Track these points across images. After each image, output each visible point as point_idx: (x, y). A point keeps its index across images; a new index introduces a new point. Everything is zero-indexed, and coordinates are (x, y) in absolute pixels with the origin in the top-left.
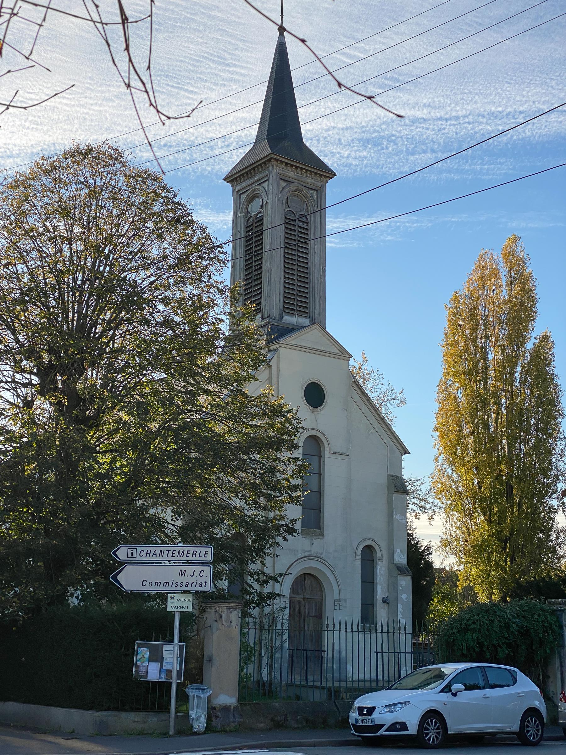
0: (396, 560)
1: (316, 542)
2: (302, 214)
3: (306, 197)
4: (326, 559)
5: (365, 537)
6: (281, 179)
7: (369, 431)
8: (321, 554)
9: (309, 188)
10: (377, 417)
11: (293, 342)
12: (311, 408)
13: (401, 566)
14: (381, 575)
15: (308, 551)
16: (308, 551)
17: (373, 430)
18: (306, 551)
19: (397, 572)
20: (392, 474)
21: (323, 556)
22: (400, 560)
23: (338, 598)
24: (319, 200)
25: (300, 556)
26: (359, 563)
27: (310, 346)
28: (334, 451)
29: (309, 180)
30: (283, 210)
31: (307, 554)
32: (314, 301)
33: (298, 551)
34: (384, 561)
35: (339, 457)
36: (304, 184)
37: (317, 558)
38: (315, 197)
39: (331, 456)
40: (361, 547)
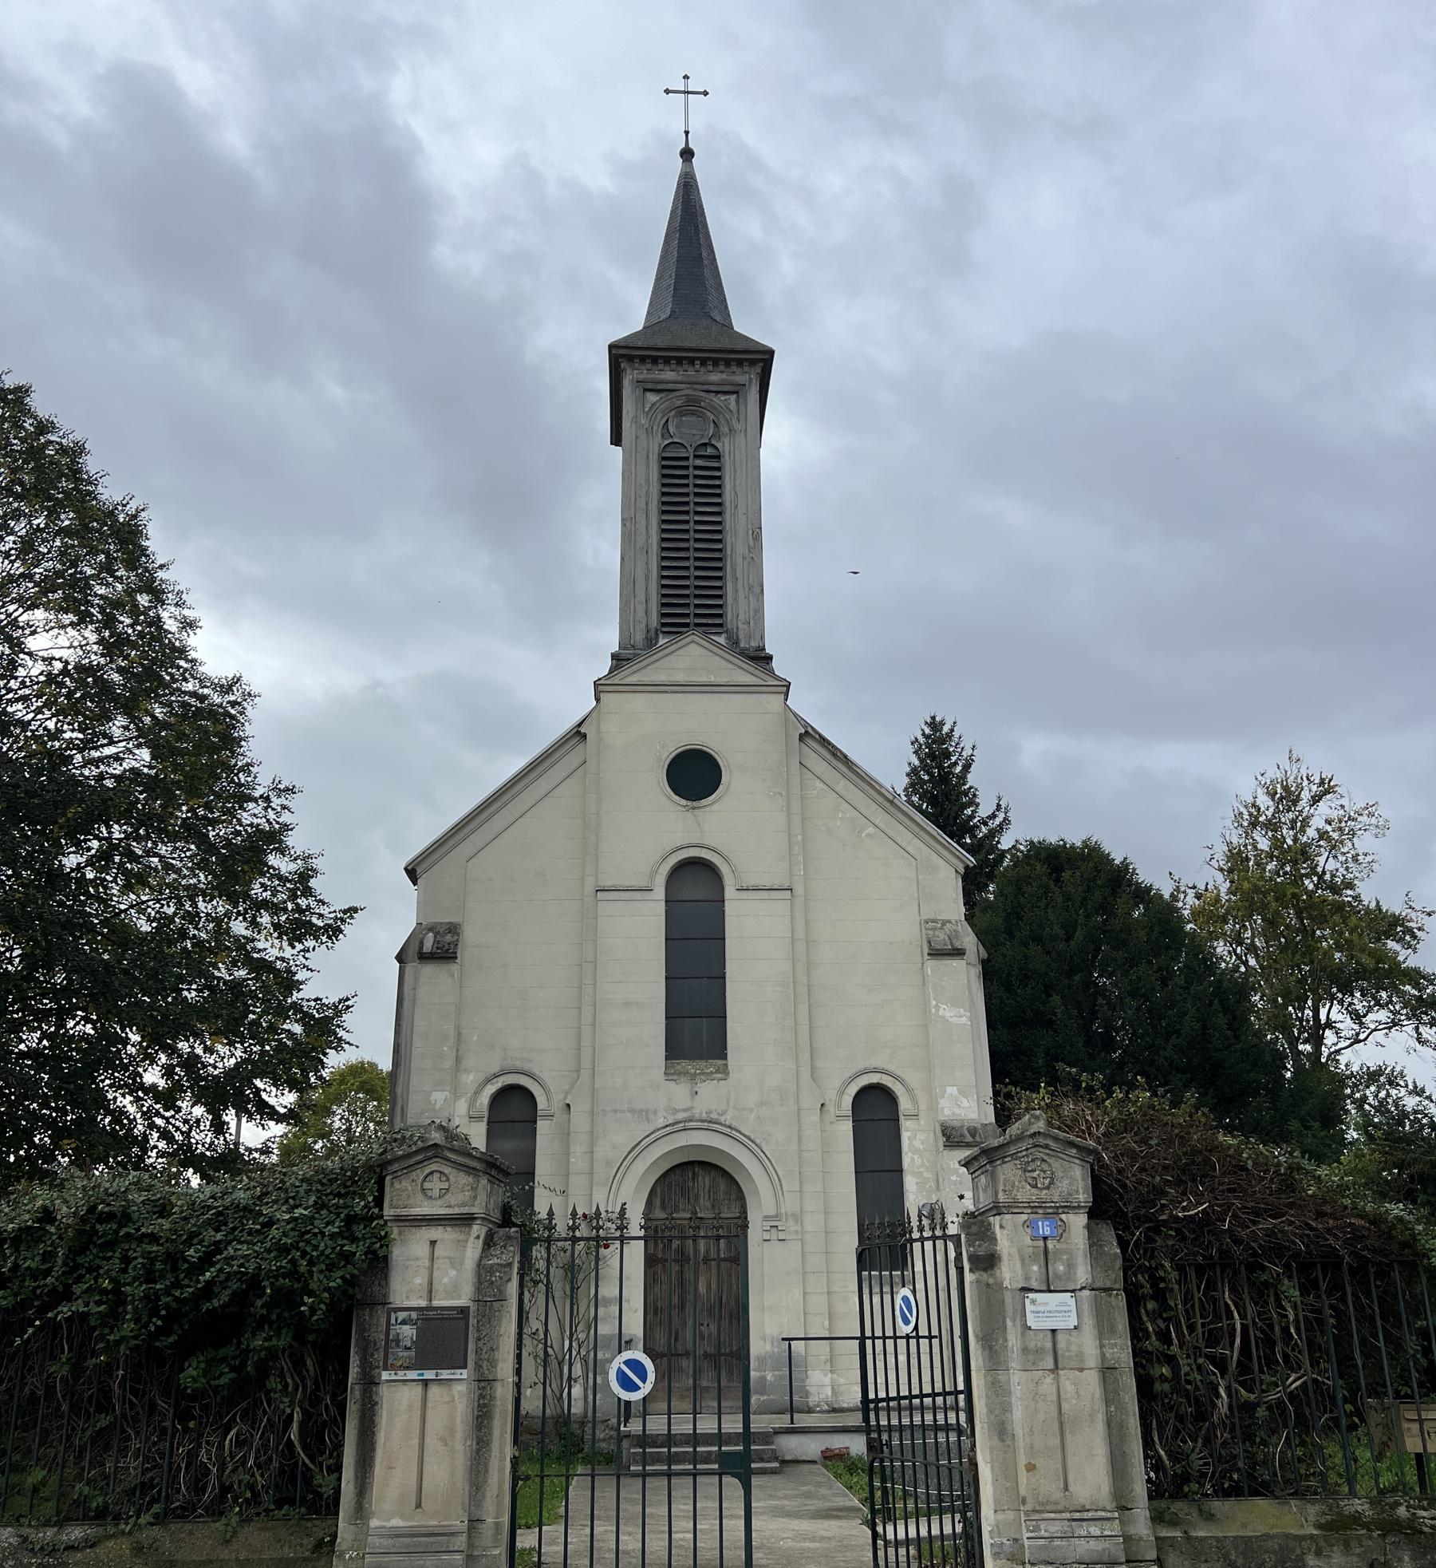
0: (947, 1112)
1: (706, 1089)
2: (705, 445)
3: (713, 409)
4: (735, 1124)
5: (861, 1065)
6: (645, 390)
7: (861, 832)
8: (724, 1113)
9: (717, 392)
10: (881, 800)
11: (634, 679)
12: (684, 802)
13: (956, 1124)
14: (917, 1151)
15: (685, 1110)
16: (685, 1110)
17: (871, 830)
18: (676, 1111)
19: (941, 1140)
20: (932, 916)
21: (727, 1118)
22: (958, 1111)
23: (773, 1212)
24: (742, 408)
25: (661, 1122)
26: (847, 1126)
27: (680, 678)
28: (751, 883)
29: (715, 377)
30: (656, 444)
31: (681, 1116)
32: (735, 599)
33: (655, 1112)
34: (922, 1115)
35: (765, 894)
36: (705, 387)
37: (710, 1124)
38: (733, 405)
39: (744, 895)
40: (853, 1089)
